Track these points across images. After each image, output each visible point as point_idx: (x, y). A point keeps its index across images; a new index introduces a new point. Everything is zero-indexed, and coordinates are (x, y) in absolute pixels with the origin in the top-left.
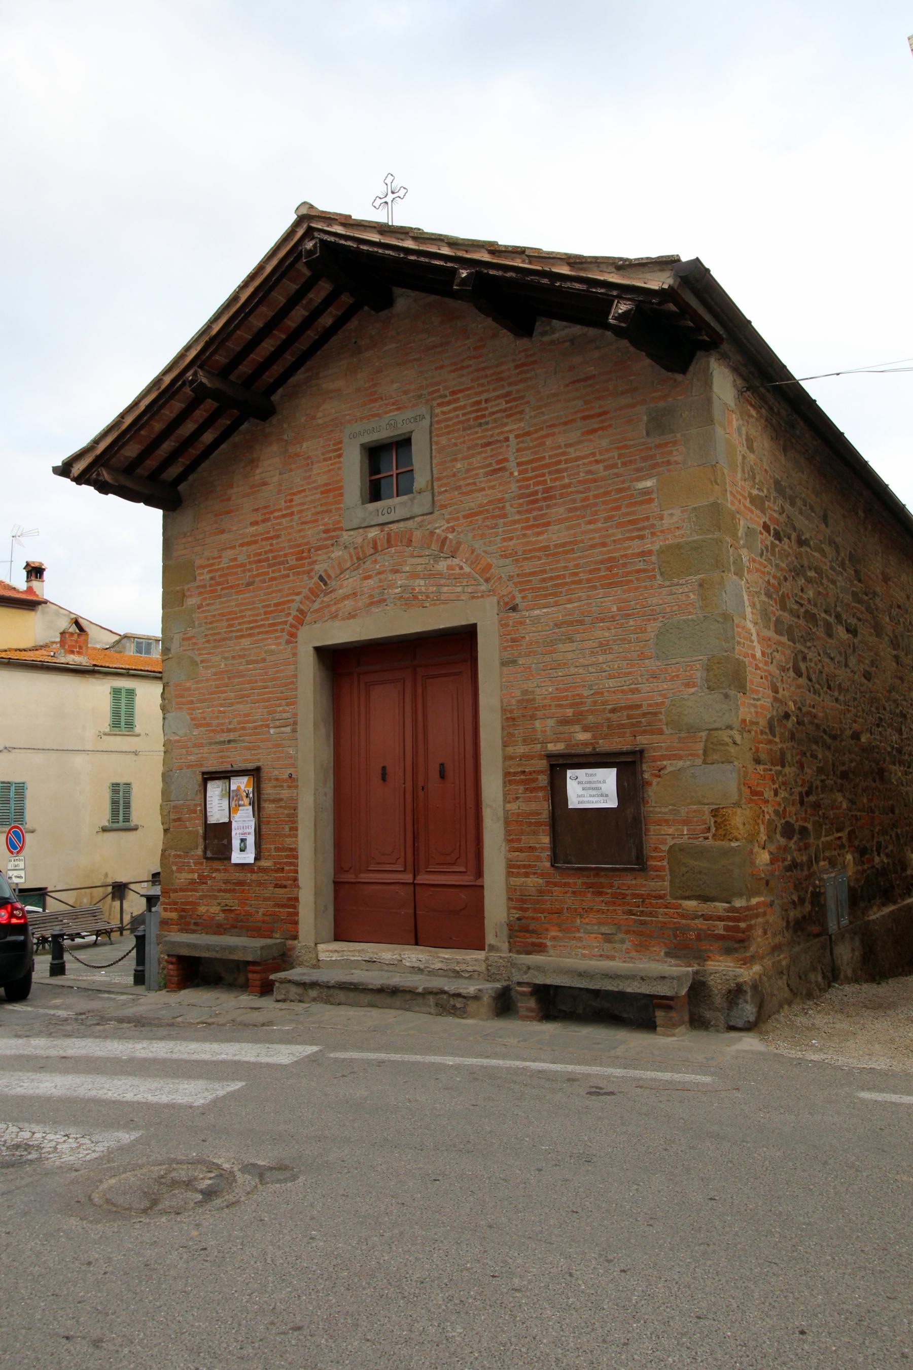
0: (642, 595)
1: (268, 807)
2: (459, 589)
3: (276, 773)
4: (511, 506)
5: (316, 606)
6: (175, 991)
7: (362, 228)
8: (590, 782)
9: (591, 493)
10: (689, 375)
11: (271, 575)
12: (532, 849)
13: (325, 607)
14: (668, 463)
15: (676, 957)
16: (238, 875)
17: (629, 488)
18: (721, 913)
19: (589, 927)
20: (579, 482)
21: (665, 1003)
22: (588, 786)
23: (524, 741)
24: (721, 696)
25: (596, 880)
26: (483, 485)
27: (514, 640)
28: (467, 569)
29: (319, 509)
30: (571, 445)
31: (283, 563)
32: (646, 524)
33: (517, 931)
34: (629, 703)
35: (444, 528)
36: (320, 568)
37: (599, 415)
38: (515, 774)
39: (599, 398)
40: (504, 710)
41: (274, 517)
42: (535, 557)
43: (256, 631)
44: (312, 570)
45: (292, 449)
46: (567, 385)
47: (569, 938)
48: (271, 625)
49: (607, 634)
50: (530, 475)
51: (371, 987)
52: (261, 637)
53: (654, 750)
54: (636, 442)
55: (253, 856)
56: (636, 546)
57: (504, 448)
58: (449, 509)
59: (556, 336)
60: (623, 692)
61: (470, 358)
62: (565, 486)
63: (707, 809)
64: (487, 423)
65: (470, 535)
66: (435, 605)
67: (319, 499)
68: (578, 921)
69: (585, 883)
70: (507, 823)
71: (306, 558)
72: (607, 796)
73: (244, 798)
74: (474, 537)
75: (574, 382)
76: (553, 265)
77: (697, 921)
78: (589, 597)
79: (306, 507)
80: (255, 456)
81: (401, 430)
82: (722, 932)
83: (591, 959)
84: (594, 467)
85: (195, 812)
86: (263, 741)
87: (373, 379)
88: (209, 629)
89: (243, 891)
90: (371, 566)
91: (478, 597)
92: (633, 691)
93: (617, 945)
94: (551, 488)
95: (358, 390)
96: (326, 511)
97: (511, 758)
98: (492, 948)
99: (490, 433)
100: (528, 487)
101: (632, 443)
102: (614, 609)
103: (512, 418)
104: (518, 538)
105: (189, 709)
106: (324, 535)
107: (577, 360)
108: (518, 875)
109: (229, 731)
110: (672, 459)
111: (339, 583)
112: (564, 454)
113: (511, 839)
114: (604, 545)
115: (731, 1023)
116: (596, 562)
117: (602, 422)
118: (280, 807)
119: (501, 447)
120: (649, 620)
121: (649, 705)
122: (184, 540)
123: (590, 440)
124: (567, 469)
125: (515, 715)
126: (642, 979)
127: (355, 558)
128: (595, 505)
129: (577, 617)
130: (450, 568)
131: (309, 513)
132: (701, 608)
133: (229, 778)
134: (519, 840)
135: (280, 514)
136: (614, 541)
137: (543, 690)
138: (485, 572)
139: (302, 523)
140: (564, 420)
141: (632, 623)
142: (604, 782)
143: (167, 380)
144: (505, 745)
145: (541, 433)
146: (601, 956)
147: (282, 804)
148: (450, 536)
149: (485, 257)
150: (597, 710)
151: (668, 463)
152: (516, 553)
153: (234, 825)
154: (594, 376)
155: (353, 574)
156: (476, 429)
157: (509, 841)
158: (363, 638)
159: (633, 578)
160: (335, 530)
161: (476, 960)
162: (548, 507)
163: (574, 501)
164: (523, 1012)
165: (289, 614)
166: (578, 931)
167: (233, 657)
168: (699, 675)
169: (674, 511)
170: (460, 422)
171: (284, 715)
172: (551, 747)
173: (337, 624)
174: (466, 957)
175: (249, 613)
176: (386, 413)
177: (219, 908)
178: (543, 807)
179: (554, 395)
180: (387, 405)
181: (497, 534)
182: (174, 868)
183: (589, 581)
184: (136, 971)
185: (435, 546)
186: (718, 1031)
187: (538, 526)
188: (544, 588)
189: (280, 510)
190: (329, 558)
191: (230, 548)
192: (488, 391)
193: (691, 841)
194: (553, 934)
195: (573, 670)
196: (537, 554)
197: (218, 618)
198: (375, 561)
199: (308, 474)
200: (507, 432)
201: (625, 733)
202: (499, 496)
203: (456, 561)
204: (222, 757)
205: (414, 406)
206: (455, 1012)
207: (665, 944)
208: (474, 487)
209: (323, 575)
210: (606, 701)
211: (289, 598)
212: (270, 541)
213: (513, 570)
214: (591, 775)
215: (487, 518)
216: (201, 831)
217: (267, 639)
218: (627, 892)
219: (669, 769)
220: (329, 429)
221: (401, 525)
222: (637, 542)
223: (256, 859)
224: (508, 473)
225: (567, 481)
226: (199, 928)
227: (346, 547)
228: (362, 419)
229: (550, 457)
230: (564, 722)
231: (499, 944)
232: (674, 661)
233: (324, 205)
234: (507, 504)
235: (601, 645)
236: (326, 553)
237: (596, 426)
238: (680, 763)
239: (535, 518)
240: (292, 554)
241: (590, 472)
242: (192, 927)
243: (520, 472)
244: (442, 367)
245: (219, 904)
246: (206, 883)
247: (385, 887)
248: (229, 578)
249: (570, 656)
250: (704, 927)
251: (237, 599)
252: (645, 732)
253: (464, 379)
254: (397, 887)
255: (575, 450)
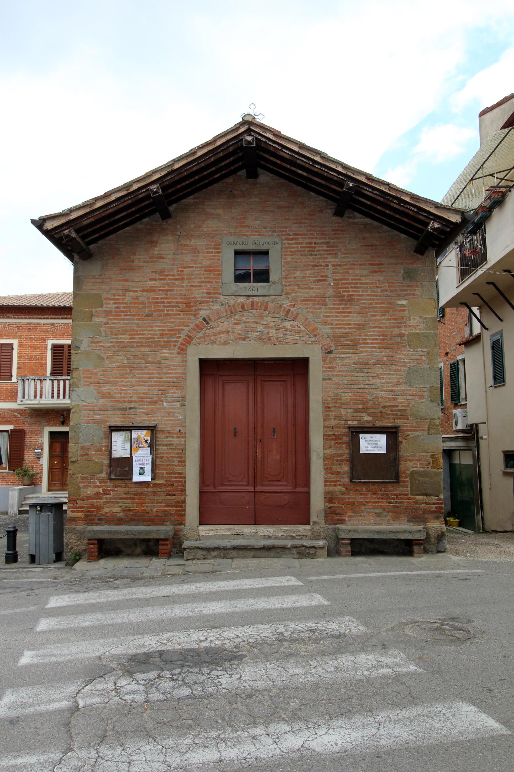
0: (399, 354)
1: (163, 449)
2: (298, 338)
3: (168, 429)
4: (329, 300)
5: (200, 335)
6: (95, 561)
7: (288, 141)
8: (372, 441)
9: (374, 302)
10: (424, 257)
11: (166, 312)
12: (339, 473)
13: (207, 336)
14: (414, 295)
15: (413, 522)
16: (139, 489)
17: (394, 302)
18: (434, 501)
19: (368, 510)
20: (368, 295)
21: (418, 542)
22: (371, 442)
23: (335, 419)
24: (436, 404)
25: (373, 487)
26: (312, 286)
27: (329, 368)
28: (302, 328)
29: (203, 280)
30: (363, 276)
31: (175, 306)
32: (402, 321)
33: (329, 514)
34: (392, 404)
35: (288, 304)
36: (203, 313)
37: (379, 265)
38: (329, 435)
39: (379, 256)
40: (324, 403)
41: (169, 279)
42: (343, 328)
43: (153, 344)
44: (198, 314)
45: (182, 241)
46: (362, 246)
47: (358, 516)
48: (165, 342)
49: (381, 370)
50: (340, 286)
51: (256, 547)
52: (157, 348)
53: (404, 427)
54: (398, 282)
55: (151, 477)
56: (396, 331)
57: (325, 270)
58: (292, 295)
59: (356, 220)
60: (389, 398)
61: (306, 219)
62: (359, 296)
63: (429, 454)
64: (316, 255)
65: (305, 311)
66: (282, 344)
67: (203, 274)
68: (363, 507)
69: (367, 489)
70: (325, 460)
71: (193, 306)
72: (381, 447)
73: (144, 443)
74: (307, 312)
75: (366, 246)
76: (402, 195)
77: (423, 505)
78: (372, 352)
79: (193, 277)
80: (154, 239)
81: (263, 247)
82: (434, 509)
83: (370, 525)
84: (375, 289)
85: (101, 450)
86: (157, 409)
87: (242, 215)
88: (114, 338)
89: (141, 498)
90: (240, 317)
91: (309, 344)
92: (394, 399)
93: (383, 518)
94: (352, 295)
95: (233, 218)
96: (208, 282)
97: (327, 427)
98: (315, 523)
99: (318, 260)
100: (339, 292)
101: (395, 282)
102: (385, 359)
103: (331, 256)
104: (333, 317)
105: (95, 386)
106: (207, 295)
107: (368, 235)
108: (330, 486)
109: (131, 402)
110: (416, 293)
111: (217, 324)
112: (360, 279)
113: (327, 468)
114: (380, 327)
115: (439, 550)
116: (376, 335)
117: (380, 268)
118: (171, 449)
119: (324, 269)
120: (403, 366)
121: (402, 406)
122: (93, 280)
123: (374, 276)
124: (361, 287)
125: (330, 405)
126: (410, 532)
127: (229, 312)
128: (376, 307)
129: (365, 360)
130: (291, 326)
131: (196, 281)
132: (428, 364)
133: (131, 431)
134: (331, 469)
135: (173, 277)
136: (386, 327)
137: (347, 395)
138: (314, 332)
139: (190, 286)
140: (359, 263)
141: (394, 366)
142: (380, 441)
143: (135, 187)
144: (324, 420)
145: (347, 267)
146: (375, 523)
147: (173, 447)
148: (292, 309)
149: (363, 179)
150: (376, 406)
151: (414, 295)
152: (332, 324)
153: (134, 459)
154: (376, 245)
155: (227, 320)
156: (309, 257)
157: (325, 469)
158: (235, 357)
159: (395, 346)
160: (214, 293)
161: (305, 530)
162: (350, 304)
163: (365, 304)
164: (344, 553)
165: (180, 337)
166: (363, 512)
167: (135, 358)
168: (426, 394)
169: (416, 317)
170: (299, 251)
171: (175, 395)
172: (350, 423)
173: (215, 346)
174: (298, 529)
175: (147, 332)
176: (251, 235)
177: (120, 509)
178: (345, 452)
179: (354, 249)
180: (252, 231)
181: (321, 313)
182: (81, 485)
183: (372, 344)
184: (7, 554)
185: (282, 313)
186: (432, 554)
187: (344, 313)
188: (347, 344)
189: (174, 275)
190: (210, 309)
191: (133, 291)
192: (316, 238)
193: (421, 469)
194: (349, 514)
195: (362, 386)
196: (344, 327)
197: (121, 332)
198: (243, 315)
199: (195, 258)
200: (327, 262)
201: (390, 418)
202: (322, 294)
203: (295, 323)
204: (123, 417)
205: (269, 236)
206: (309, 556)
207: (407, 516)
208: (307, 286)
209: (206, 318)
210: (380, 402)
211: (180, 328)
212: (165, 292)
213: (330, 332)
214: (373, 437)
215: (315, 304)
216: (106, 462)
217: (162, 350)
218: (389, 493)
219: (411, 436)
220: (211, 235)
221: (261, 298)
222: (397, 329)
223: (152, 479)
224: (328, 283)
225: (361, 293)
226: (103, 522)
227: (222, 305)
228: (234, 235)
229: (352, 280)
230: (357, 411)
231: (319, 521)
232: (414, 386)
233: (260, 120)
234: (327, 299)
235: (378, 375)
236: (208, 306)
237: (377, 270)
238: (416, 434)
239: (343, 309)
240: (183, 302)
241: (373, 291)
242: (96, 521)
243: (335, 284)
244: (288, 219)
245: (120, 507)
246: (110, 494)
247: (238, 494)
248: (132, 309)
249: (361, 379)
250: (426, 508)
251: (138, 323)
252: (400, 418)
253: (301, 229)
254: (243, 494)
255: (366, 279)
